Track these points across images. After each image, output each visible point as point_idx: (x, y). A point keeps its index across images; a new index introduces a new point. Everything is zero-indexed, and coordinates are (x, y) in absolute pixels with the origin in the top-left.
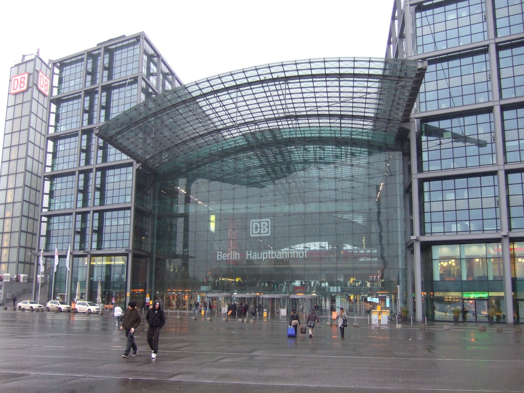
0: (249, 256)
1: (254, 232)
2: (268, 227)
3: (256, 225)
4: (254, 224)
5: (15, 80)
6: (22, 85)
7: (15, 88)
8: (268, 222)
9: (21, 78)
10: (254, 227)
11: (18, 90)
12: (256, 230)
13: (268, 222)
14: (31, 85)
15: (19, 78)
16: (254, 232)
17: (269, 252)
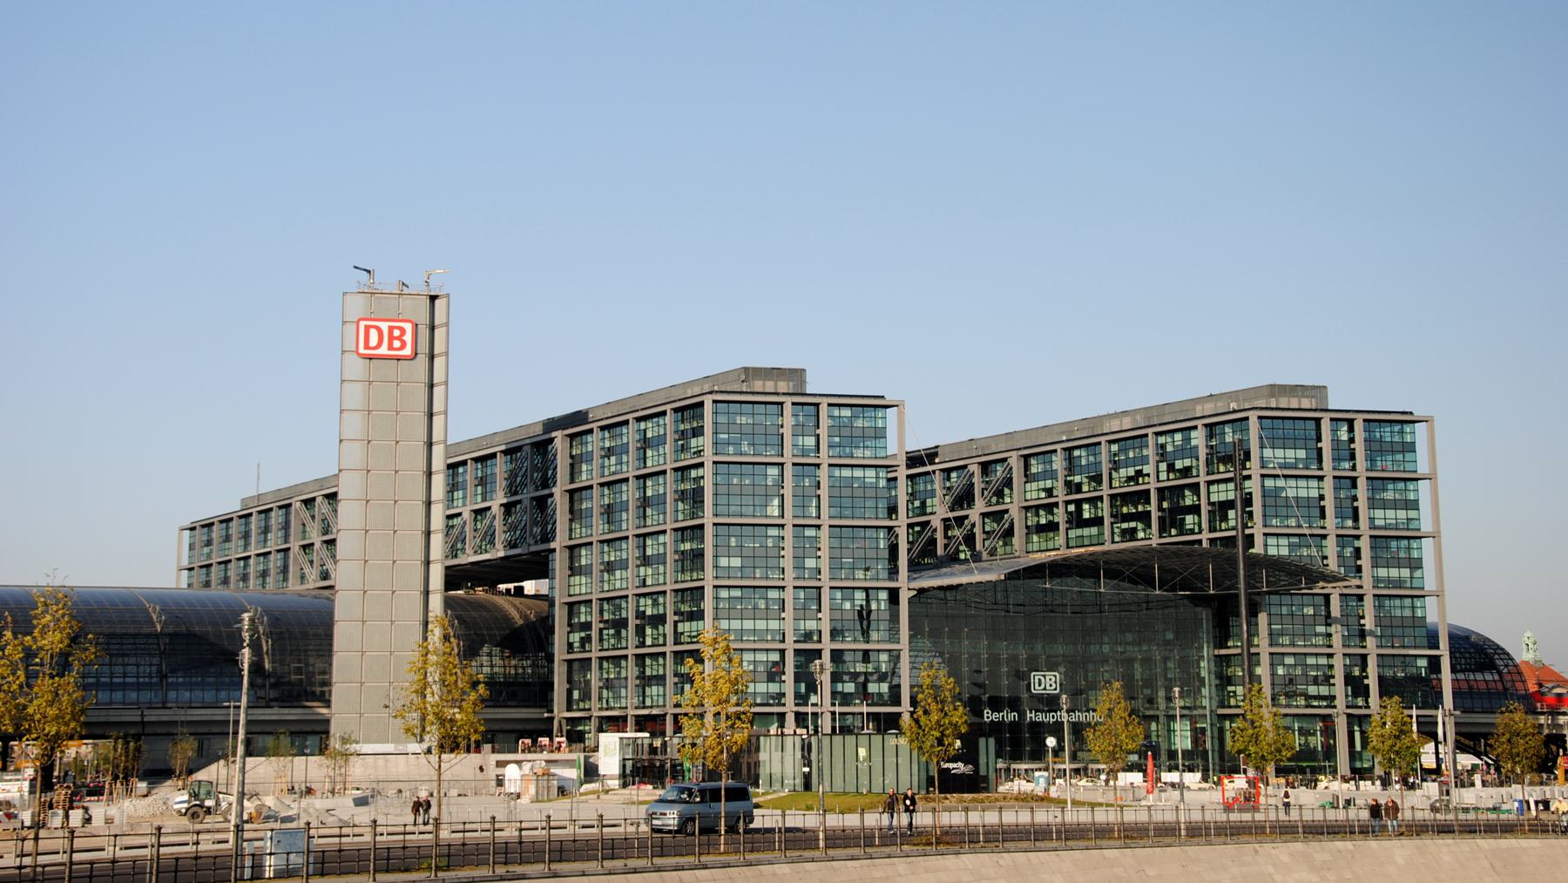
0: (1031, 718)
1: (1037, 687)
2: (1056, 682)
3: (1040, 680)
4: (1037, 678)
5: (367, 328)
6: (397, 344)
7: (374, 341)
8: (1055, 676)
9: (391, 329)
10: (1037, 681)
11: (384, 350)
12: (1040, 685)
13: (1055, 676)
14: (423, 347)
15: (384, 326)
16: (1037, 687)
17: (1059, 713)
